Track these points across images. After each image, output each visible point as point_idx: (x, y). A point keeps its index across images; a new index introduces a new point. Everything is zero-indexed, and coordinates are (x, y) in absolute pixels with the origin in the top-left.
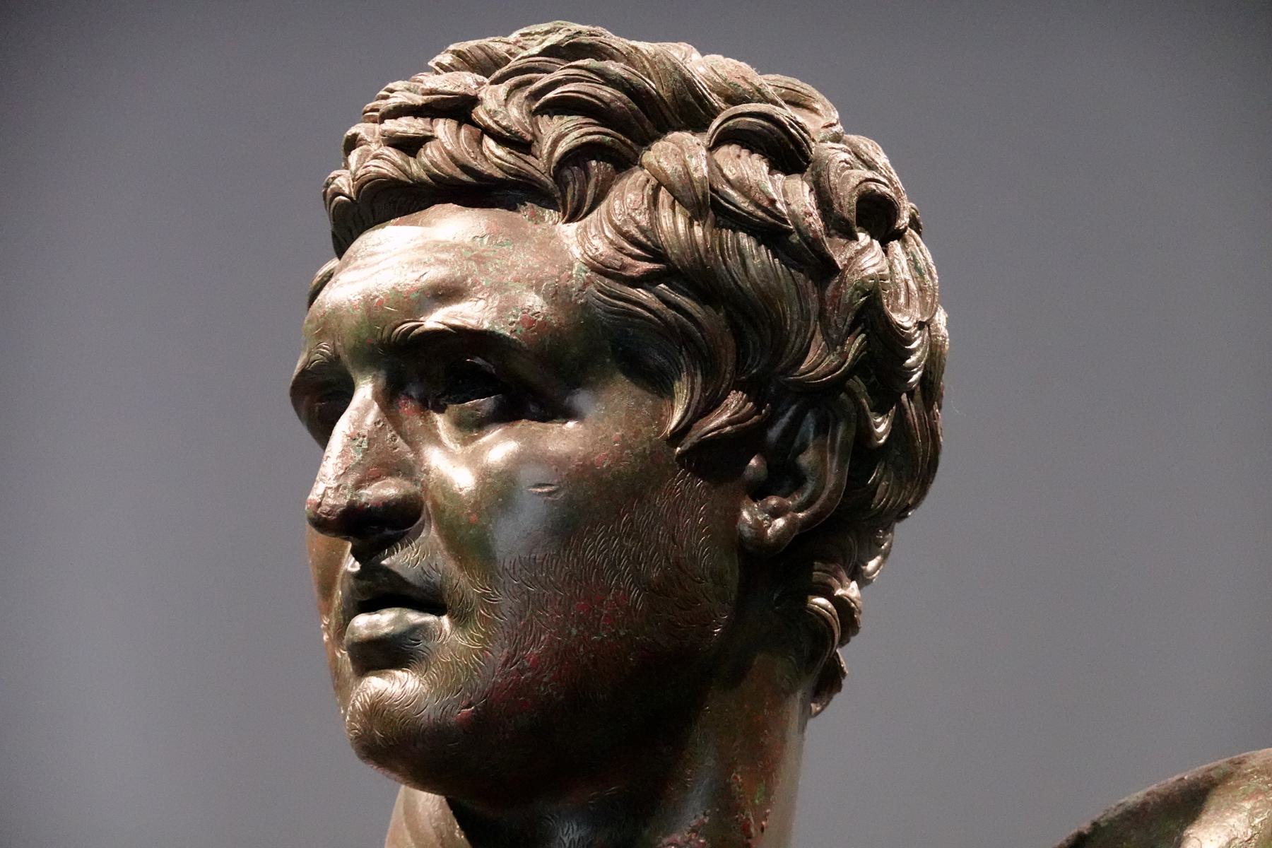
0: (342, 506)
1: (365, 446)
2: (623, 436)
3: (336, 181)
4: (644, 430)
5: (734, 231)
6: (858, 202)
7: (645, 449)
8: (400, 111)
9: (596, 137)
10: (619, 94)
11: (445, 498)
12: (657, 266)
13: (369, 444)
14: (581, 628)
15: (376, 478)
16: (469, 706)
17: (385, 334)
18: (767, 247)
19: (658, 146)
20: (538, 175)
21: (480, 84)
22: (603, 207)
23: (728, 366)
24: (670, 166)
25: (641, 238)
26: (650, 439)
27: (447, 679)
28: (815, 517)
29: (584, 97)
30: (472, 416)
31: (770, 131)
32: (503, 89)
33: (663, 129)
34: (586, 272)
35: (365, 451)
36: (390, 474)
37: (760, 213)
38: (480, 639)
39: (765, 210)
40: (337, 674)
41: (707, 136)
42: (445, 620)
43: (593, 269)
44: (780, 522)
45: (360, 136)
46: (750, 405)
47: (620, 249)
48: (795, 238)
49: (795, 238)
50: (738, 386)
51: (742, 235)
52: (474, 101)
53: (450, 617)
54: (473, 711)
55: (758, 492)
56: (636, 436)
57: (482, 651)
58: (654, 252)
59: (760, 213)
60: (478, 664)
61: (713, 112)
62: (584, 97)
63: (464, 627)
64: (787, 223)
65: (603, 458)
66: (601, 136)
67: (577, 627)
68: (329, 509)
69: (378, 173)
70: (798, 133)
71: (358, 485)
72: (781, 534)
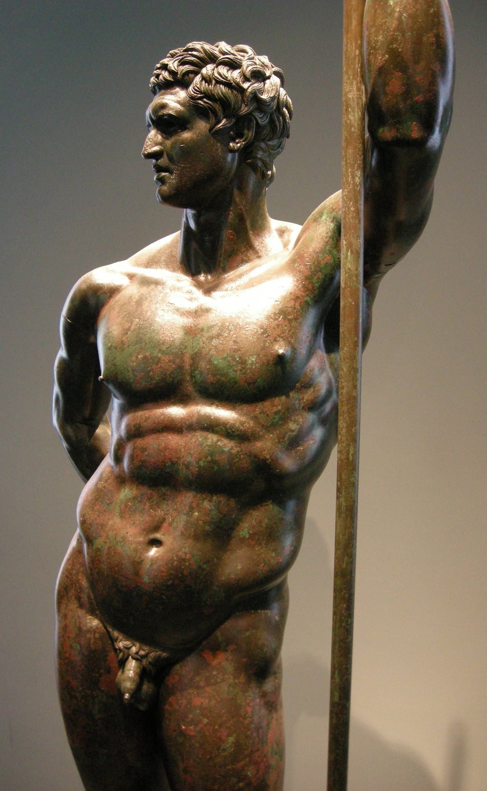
4: (203, 130)
12: (202, 95)
28: (247, 143)
37: (224, 80)
39: (225, 79)
50: (224, 118)
51: (221, 86)
55: (233, 140)
58: (201, 92)
59: (224, 80)
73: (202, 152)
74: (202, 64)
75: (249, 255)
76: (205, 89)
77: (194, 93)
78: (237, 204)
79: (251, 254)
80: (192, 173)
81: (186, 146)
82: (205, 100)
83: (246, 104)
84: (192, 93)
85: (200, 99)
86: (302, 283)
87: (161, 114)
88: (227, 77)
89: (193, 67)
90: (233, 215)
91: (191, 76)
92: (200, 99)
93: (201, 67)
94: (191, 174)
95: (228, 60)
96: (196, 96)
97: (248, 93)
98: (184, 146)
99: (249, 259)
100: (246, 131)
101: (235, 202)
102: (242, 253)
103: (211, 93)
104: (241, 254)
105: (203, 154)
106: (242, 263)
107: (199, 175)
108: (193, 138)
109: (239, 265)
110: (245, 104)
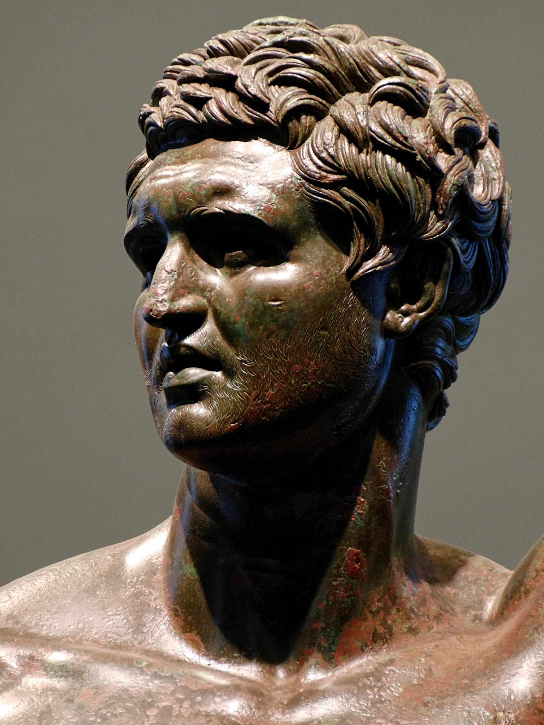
0: (165, 311)
1: (176, 277)
2: (320, 273)
3: (152, 115)
5: (384, 154)
6: (455, 133)
7: (332, 280)
8: (191, 79)
9: (305, 101)
10: (319, 74)
11: (221, 306)
13: (178, 275)
14: (297, 380)
15: (182, 296)
17: (187, 212)
18: (403, 164)
19: (342, 101)
20: (273, 123)
21: (237, 63)
22: (309, 141)
23: (380, 233)
24: (348, 118)
25: (331, 161)
26: (336, 274)
27: (222, 407)
30: (235, 260)
31: (404, 93)
32: (253, 69)
33: (344, 91)
34: (300, 180)
35: (176, 280)
36: (189, 293)
37: (398, 145)
38: (241, 386)
39: (401, 143)
40: (153, 404)
41: (367, 95)
44: (407, 320)
45: (165, 90)
46: (391, 254)
47: (319, 167)
48: (419, 158)
49: (419, 158)
50: (384, 243)
52: (235, 78)
54: (237, 425)
56: (327, 273)
57: (242, 392)
58: (338, 170)
60: (240, 399)
61: (372, 81)
63: (232, 379)
64: (414, 150)
65: (310, 285)
66: (309, 100)
67: (295, 379)
68: (157, 313)
69: (179, 116)
70: (423, 94)
71: (173, 300)
72: (409, 327)
73: (324, 328)
74: (215, 55)
75: (389, 622)
76: (352, 164)
77: (319, 167)
78: (380, 476)
79: (394, 621)
80: (293, 382)
81: (284, 307)
83: (441, 212)
84: (313, 168)
85: (335, 186)
87: (218, 210)
88: (406, 138)
89: (314, 97)
90: (366, 506)
91: (306, 120)
92: (335, 186)
93: (332, 100)
94: (290, 384)
95: (401, 88)
96: (326, 177)
97: (450, 185)
99: (391, 634)
100: (429, 285)
101: (376, 472)
102: (374, 614)
103: (366, 176)
104: (369, 616)
105: (326, 333)
106: (374, 641)
107: (308, 388)
108: (304, 289)
109: (366, 646)
110: (436, 213)
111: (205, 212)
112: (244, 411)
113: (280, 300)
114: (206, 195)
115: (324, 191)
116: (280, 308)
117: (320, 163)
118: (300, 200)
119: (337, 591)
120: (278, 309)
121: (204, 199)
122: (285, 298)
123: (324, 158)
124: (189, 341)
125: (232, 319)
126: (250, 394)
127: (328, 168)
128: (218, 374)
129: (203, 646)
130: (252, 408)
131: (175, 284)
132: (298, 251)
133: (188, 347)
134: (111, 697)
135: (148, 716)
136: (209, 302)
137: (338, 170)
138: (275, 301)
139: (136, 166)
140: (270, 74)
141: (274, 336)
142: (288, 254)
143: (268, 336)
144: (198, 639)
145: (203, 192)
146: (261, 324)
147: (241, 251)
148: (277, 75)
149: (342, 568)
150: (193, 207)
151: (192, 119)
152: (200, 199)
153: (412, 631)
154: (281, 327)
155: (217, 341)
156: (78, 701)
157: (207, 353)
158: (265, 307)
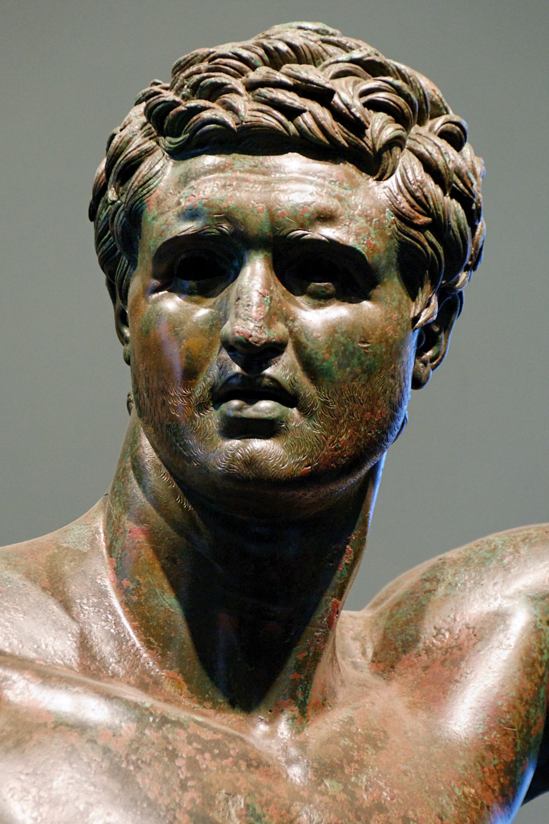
1: (269, 301)
11: (308, 340)
16: (307, 466)
17: (285, 232)
20: (368, 149)
25: (423, 200)
29: (392, 103)
30: (323, 292)
35: (269, 305)
42: (295, 411)
43: (397, 215)
52: (331, 93)
53: (300, 410)
54: (309, 469)
58: (427, 212)
62: (392, 103)
81: (370, 350)
82: (428, 233)
86: (499, 781)
92: (421, 228)
98: (367, 348)
111: (305, 237)
112: (319, 455)
113: (368, 343)
114: (309, 219)
115: (414, 232)
116: (367, 351)
117: (412, 200)
118: (391, 238)
119: (318, 643)
120: (365, 352)
121: (307, 223)
122: (372, 341)
123: (418, 197)
124: (268, 371)
125: (320, 356)
126: (327, 439)
127: (421, 209)
128: (294, 411)
129: (186, 687)
130: (326, 453)
131: (269, 309)
132: (379, 292)
133: (272, 379)
134: (132, 741)
135: (180, 768)
136: (291, 332)
137: (427, 212)
138: (364, 342)
139: (141, 153)
140: (363, 94)
141: (357, 380)
142: (371, 293)
143: (353, 380)
144: (180, 678)
145: (307, 215)
146: (348, 365)
147: (330, 284)
148: (370, 97)
149: (325, 620)
150: (293, 228)
151: (281, 128)
152: (302, 222)
153: (34, 618)
154: (364, 372)
155: (298, 376)
156: (101, 742)
157: (289, 388)
158: (354, 348)
